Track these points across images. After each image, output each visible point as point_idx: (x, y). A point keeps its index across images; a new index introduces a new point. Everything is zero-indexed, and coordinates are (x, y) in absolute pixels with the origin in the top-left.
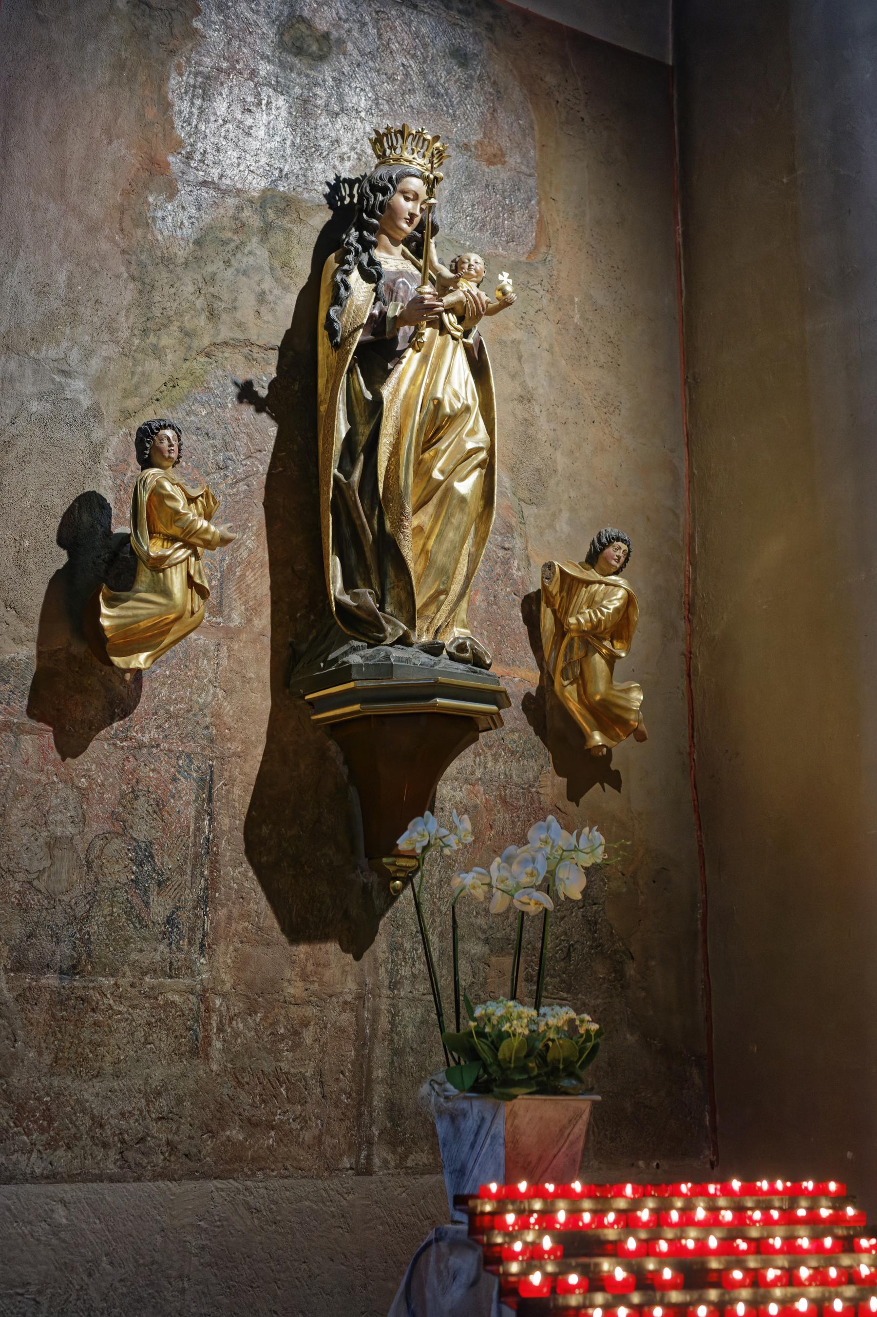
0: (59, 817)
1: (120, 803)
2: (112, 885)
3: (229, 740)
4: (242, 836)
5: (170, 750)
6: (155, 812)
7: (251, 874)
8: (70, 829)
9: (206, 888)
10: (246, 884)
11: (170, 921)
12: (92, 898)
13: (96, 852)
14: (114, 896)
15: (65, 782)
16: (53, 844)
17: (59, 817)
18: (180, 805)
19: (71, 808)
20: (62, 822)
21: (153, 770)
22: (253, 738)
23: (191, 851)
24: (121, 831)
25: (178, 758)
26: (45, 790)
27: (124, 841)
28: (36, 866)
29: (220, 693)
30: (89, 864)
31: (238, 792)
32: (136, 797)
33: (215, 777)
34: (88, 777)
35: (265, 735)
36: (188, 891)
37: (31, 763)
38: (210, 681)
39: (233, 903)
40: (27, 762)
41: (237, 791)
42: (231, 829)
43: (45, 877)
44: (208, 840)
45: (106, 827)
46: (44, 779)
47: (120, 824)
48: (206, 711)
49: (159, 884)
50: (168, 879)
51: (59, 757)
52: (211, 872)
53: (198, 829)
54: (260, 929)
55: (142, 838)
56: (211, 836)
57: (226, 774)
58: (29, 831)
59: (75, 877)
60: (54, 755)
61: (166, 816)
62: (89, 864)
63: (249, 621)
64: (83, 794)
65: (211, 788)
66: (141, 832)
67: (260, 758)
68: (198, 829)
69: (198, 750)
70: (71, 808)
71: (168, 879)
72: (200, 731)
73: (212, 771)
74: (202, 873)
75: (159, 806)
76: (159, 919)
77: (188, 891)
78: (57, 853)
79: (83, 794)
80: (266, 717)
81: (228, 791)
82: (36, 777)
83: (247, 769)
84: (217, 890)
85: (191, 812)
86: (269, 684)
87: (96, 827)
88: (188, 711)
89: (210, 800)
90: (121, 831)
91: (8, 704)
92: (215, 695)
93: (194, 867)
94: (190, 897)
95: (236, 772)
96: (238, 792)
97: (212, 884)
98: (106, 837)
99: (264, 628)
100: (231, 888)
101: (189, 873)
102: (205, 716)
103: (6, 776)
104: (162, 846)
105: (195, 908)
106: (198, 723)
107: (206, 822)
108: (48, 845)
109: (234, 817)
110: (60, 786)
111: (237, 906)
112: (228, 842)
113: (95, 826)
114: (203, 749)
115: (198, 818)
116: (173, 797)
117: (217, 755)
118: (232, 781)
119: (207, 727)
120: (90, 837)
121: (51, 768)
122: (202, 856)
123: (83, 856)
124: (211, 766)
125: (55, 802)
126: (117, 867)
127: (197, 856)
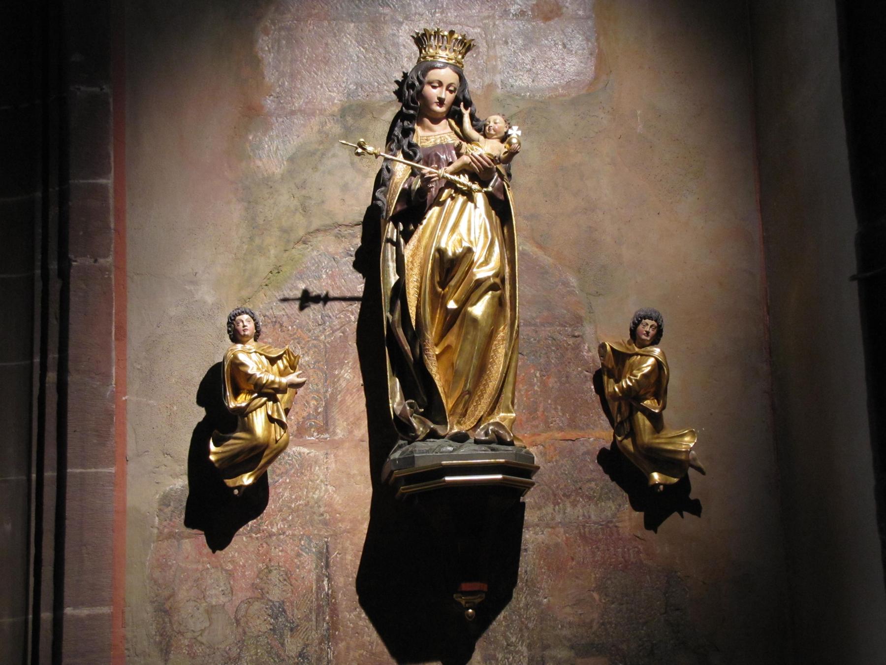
0: (213, 592)
1: (258, 577)
2: (256, 633)
3: (340, 521)
4: (355, 589)
5: (294, 535)
6: (285, 580)
7: (364, 615)
8: (222, 599)
9: (328, 629)
10: (361, 623)
11: (301, 655)
12: (241, 643)
13: (242, 612)
14: (258, 641)
15: (217, 567)
16: (210, 611)
17: (213, 592)
18: (304, 573)
19: (222, 584)
20: (216, 595)
21: (281, 551)
22: (359, 517)
23: (315, 604)
24: (260, 596)
25: (300, 540)
26: (202, 575)
27: (263, 603)
28: (199, 626)
29: (330, 488)
30: (238, 621)
31: (350, 558)
32: (270, 571)
33: (330, 549)
34: (232, 561)
35: (368, 514)
36: (314, 632)
37: (190, 557)
38: (322, 481)
39: (351, 638)
40: (187, 557)
41: (349, 557)
42: (346, 585)
43: (206, 633)
44: (328, 594)
45: (249, 594)
46: (200, 567)
47: (259, 592)
48: (321, 503)
49: (292, 630)
50: (298, 626)
51: (210, 551)
52: (331, 617)
53: (320, 588)
54: (373, 654)
55: (276, 599)
56: (330, 592)
57: (340, 546)
58: (192, 603)
59: (228, 632)
60: (207, 550)
61: (293, 581)
62: (238, 621)
63: (351, 432)
64: (230, 574)
65: (327, 558)
66: (275, 595)
67: (366, 531)
68: (320, 588)
69: (316, 532)
70: (222, 584)
71: (298, 626)
72: (316, 517)
73: (327, 547)
74: (324, 619)
75: (288, 577)
76: (293, 654)
77: (314, 632)
78: (214, 616)
79: (230, 574)
80: (369, 501)
81: (342, 559)
82: (195, 566)
83: (356, 540)
84: (337, 629)
85: (313, 576)
86: (369, 476)
87: (241, 596)
88: (306, 505)
89: (327, 566)
90: (260, 596)
91: (171, 520)
92: (327, 490)
93: (317, 615)
94: (315, 636)
95: (348, 544)
96: (350, 558)
97: (334, 625)
98: (249, 602)
99: (363, 435)
100: (348, 627)
101: (314, 619)
102: (319, 507)
103: (173, 568)
104: (292, 603)
105: (320, 644)
106: (314, 513)
107: (325, 583)
108: (207, 611)
109: (348, 576)
110: (213, 571)
111: (354, 639)
112: (344, 594)
113: (240, 595)
114: (320, 530)
115: (319, 580)
116: (298, 567)
117: (332, 533)
118: (344, 551)
119: (322, 515)
120: (237, 603)
121: (205, 559)
122: (323, 606)
123: (232, 617)
124: (326, 542)
125: (209, 582)
126: (258, 622)
127: (319, 607)
